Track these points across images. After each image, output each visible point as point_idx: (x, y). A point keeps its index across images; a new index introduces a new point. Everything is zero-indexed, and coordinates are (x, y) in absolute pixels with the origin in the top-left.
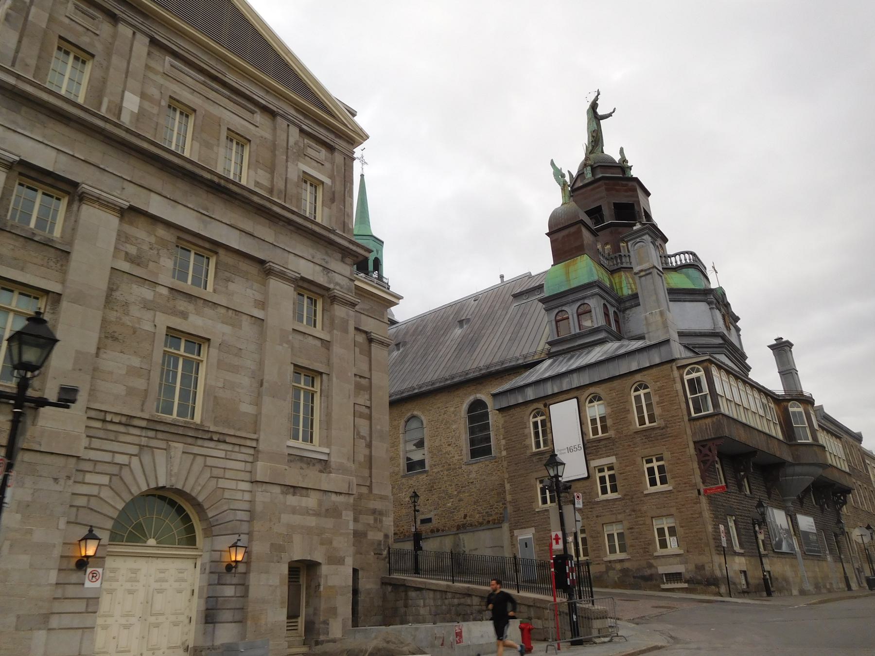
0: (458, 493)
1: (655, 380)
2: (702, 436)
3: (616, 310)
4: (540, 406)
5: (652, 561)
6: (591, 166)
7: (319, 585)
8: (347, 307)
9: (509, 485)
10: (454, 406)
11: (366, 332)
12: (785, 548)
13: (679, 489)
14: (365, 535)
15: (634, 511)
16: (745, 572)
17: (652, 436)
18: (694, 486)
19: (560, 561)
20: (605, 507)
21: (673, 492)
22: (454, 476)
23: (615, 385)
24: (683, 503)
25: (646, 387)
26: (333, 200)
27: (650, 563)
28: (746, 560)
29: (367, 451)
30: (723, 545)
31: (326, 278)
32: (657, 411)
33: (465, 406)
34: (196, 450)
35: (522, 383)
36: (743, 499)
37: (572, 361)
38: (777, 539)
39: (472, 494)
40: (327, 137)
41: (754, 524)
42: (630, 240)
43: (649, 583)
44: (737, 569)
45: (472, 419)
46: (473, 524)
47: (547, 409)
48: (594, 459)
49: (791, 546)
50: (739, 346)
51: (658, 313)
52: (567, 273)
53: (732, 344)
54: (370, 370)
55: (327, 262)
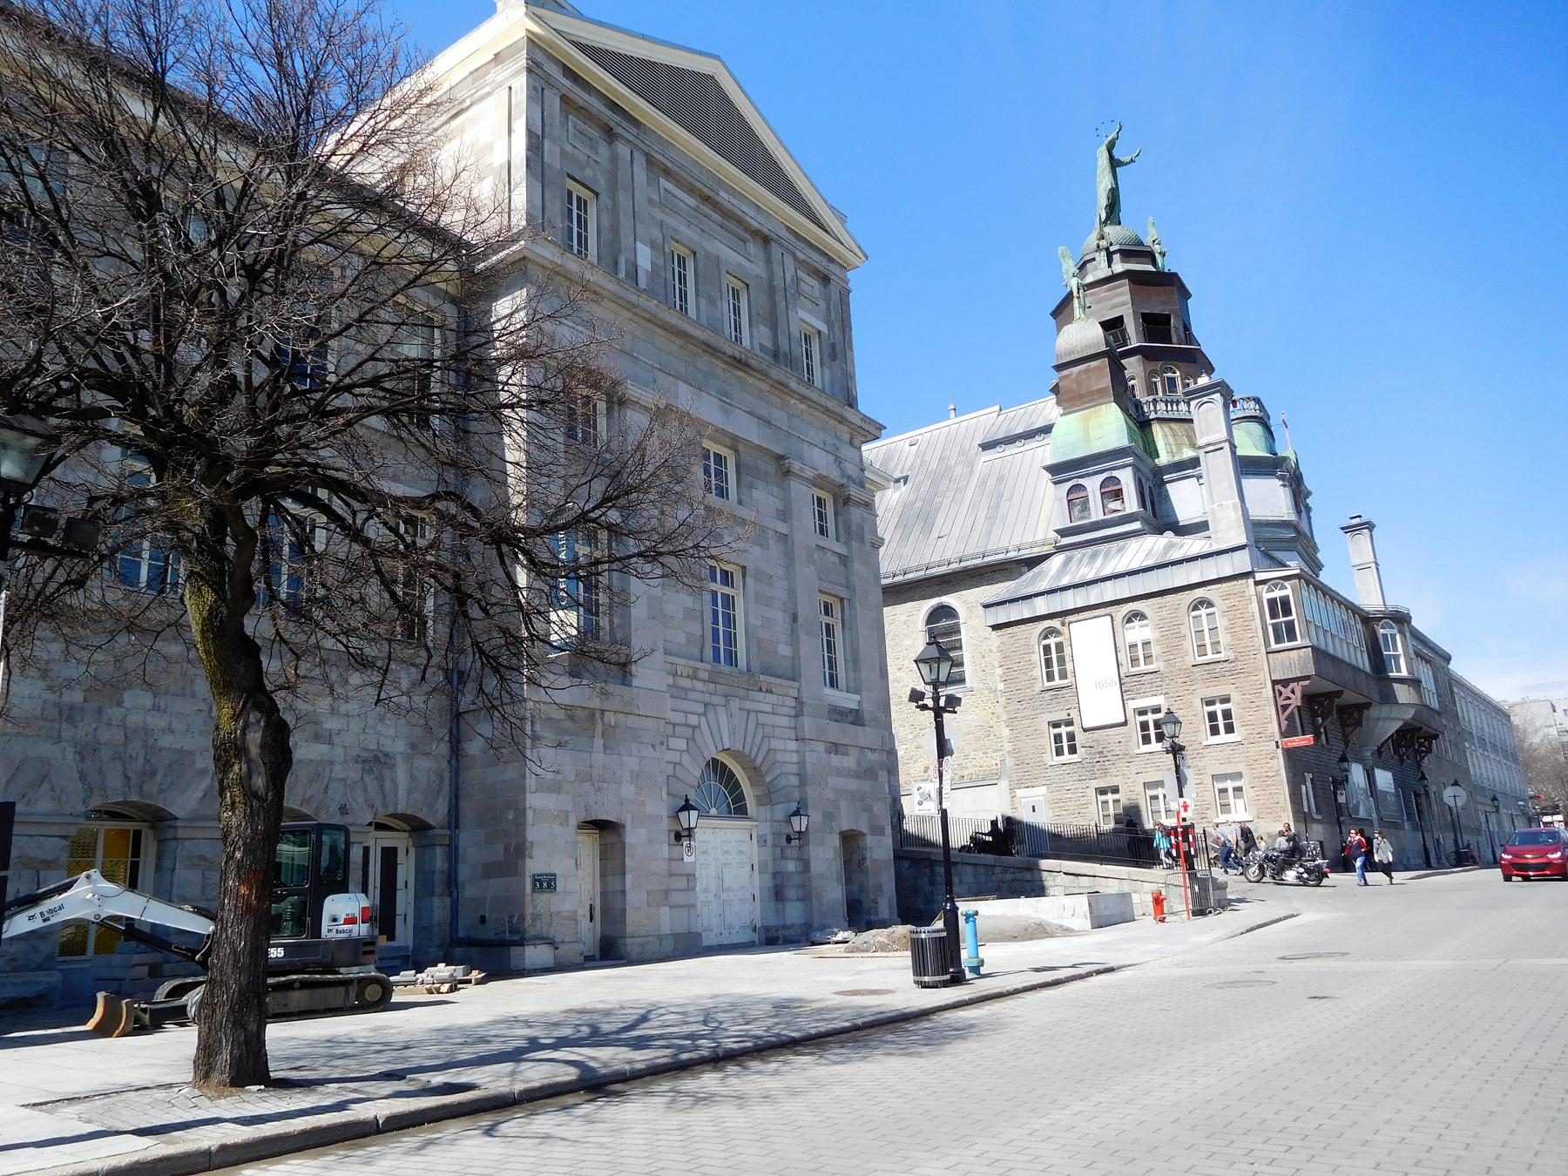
4: (1056, 623)
6: (1107, 249)
7: (864, 859)
9: (1008, 729)
10: (907, 614)
25: (1210, 604)
32: (1224, 638)
34: (749, 705)
37: (1099, 561)
50: (1308, 532)
52: (1087, 429)
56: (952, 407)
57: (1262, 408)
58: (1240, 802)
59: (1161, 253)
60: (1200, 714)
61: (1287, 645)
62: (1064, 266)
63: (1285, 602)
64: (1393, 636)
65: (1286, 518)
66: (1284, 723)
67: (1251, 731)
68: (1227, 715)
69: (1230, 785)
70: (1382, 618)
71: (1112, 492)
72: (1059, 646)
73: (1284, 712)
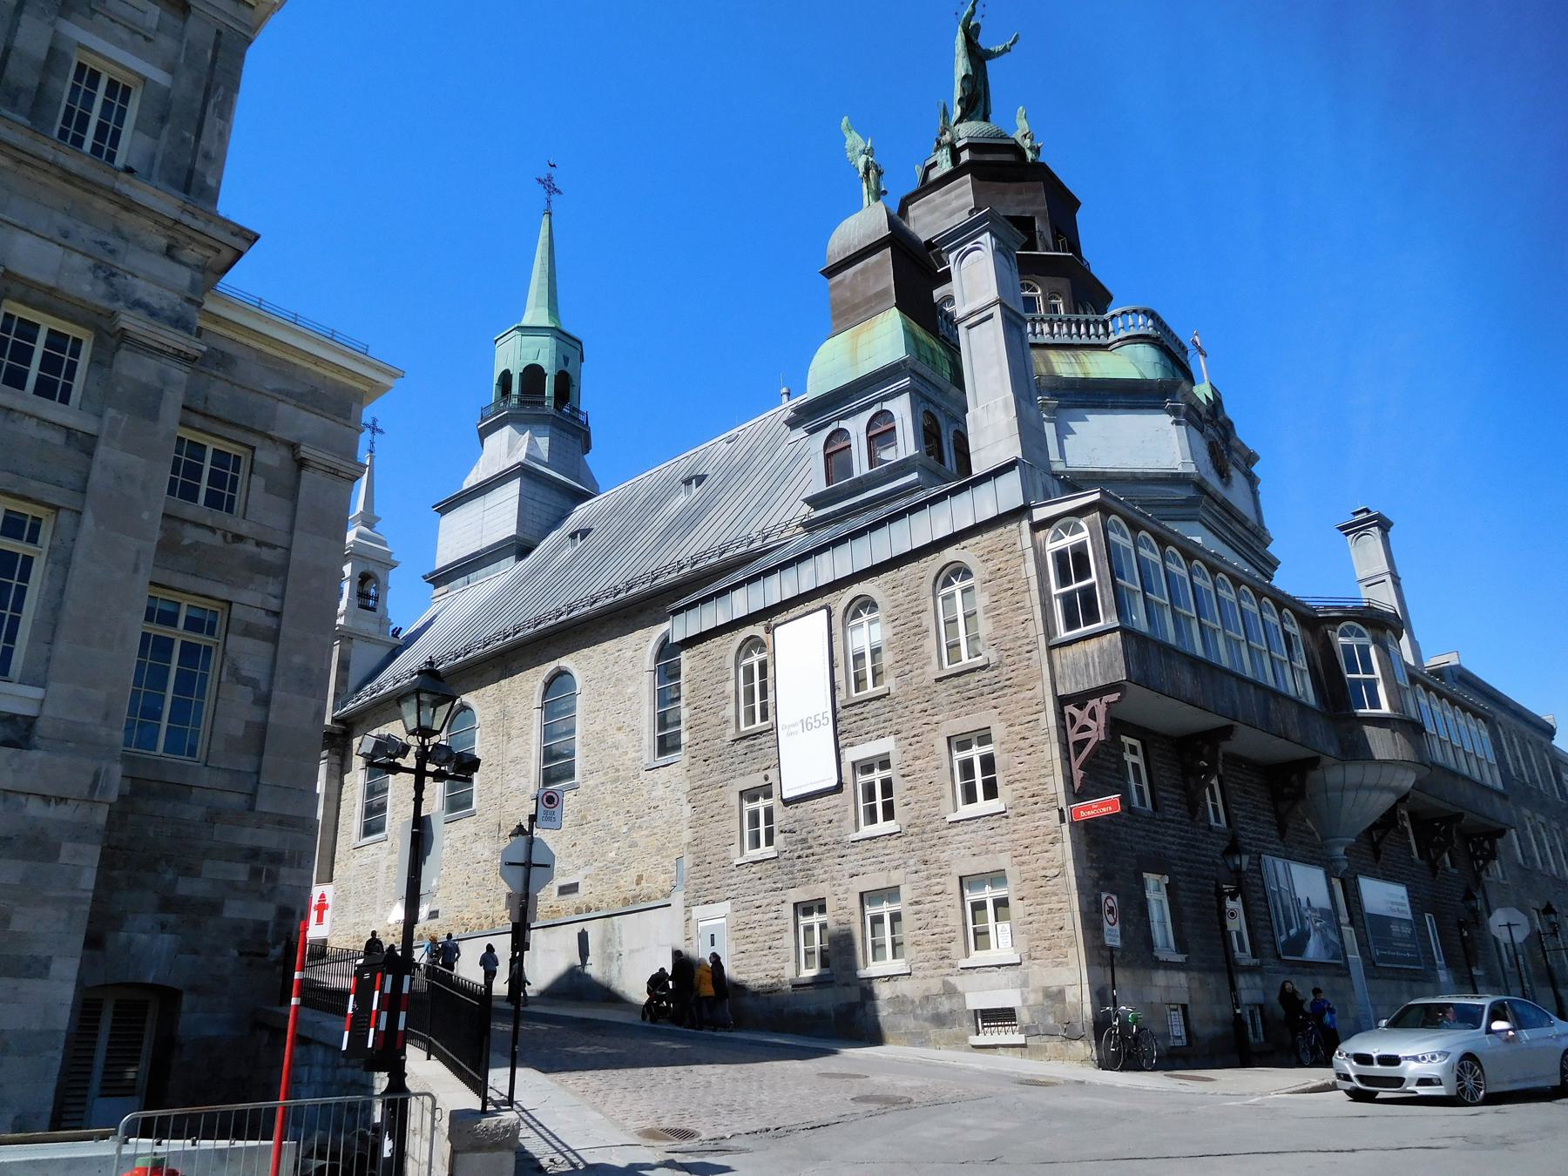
1: (985, 558)
2: (1077, 683)
4: (758, 630)
5: (951, 979)
6: (952, 145)
8: (164, 360)
9: (690, 806)
10: (634, 647)
11: (293, 447)
12: (1313, 951)
13: (1022, 810)
14: (215, 908)
15: (925, 862)
16: (1184, 1007)
17: (971, 687)
18: (1052, 800)
20: (868, 854)
21: (1007, 817)
22: (625, 794)
24: (1027, 842)
25: (967, 573)
26: (163, 119)
28: (1190, 980)
29: (256, 714)
30: (1108, 942)
31: (102, 288)
32: (985, 627)
33: (651, 647)
36: (1201, 837)
38: (1293, 932)
39: (655, 831)
41: (1220, 896)
42: (950, 250)
43: (947, 1031)
44: (1157, 1000)
46: (653, 896)
47: (770, 636)
48: (852, 745)
49: (1341, 951)
50: (1252, 517)
51: (1000, 404)
52: (854, 349)
53: (1227, 507)
54: (291, 532)
55: (112, 252)
56: (784, 390)
57: (1159, 322)
58: (1004, 926)
59: (1031, 148)
60: (946, 765)
61: (1083, 630)
62: (849, 143)
63: (1080, 554)
65: (1180, 470)
66: (1078, 775)
67: (1019, 793)
68: (988, 763)
69: (988, 894)
70: (1339, 620)
71: (881, 435)
72: (763, 666)
73: (1078, 754)
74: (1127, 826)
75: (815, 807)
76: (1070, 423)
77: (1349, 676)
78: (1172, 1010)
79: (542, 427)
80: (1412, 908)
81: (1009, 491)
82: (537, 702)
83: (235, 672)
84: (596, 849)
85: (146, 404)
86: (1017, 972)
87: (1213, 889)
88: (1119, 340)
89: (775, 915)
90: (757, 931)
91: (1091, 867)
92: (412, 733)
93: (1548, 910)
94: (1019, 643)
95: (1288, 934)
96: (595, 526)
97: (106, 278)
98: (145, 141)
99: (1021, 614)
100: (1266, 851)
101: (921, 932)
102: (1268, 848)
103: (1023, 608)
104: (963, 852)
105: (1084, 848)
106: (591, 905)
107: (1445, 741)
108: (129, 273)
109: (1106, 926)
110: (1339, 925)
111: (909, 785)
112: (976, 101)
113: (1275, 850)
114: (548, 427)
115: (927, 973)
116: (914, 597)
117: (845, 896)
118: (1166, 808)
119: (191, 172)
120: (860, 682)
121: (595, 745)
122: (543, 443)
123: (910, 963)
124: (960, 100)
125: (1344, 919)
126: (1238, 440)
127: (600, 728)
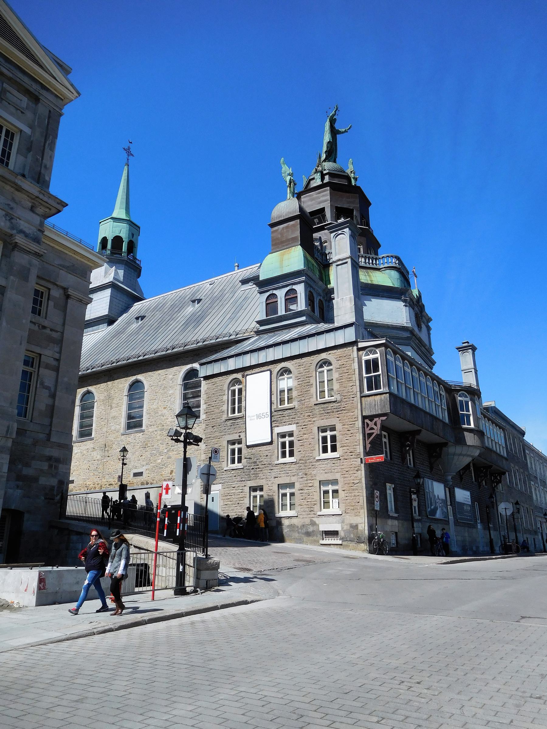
0: (168, 451)
1: (338, 359)
2: (371, 411)
3: (322, 299)
4: (239, 376)
5: (314, 519)
6: (322, 172)
8: (30, 256)
9: (205, 445)
11: (65, 289)
13: (346, 457)
14: (36, 480)
15: (306, 474)
16: (396, 533)
17: (329, 408)
18: (358, 455)
19: (173, 512)
20: (282, 470)
21: (340, 460)
23: (304, 360)
24: (347, 470)
25: (330, 364)
26: (29, 149)
27: (313, 520)
29: (50, 401)
30: (376, 508)
31: (8, 223)
32: (336, 386)
35: (226, 355)
38: (432, 507)
39: (180, 452)
40: (34, 87)
41: (411, 492)
43: (311, 538)
45: (186, 387)
48: (278, 426)
49: (446, 515)
50: (427, 343)
52: (281, 261)
53: (420, 340)
54: (64, 324)
55: (12, 208)
56: (237, 264)
57: (401, 262)
58: (336, 500)
59: (354, 178)
60: (317, 437)
61: (374, 391)
62: (283, 169)
63: (375, 361)
64: (467, 403)
65: (405, 325)
66: (368, 446)
67: (346, 451)
68: (334, 438)
69: (330, 488)
70: (459, 391)
71: (291, 298)
72: (240, 391)
73: (369, 438)
74: (382, 466)
75: (260, 449)
76: (365, 302)
77: (461, 412)
78: (392, 534)
79: (121, 265)
80: (471, 500)
81: (350, 335)
82: (126, 393)
83: (42, 384)
84: (152, 458)
85: (24, 275)
86: (340, 518)
87: (408, 490)
88: (385, 268)
89: (241, 491)
90: (233, 497)
91: (370, 481)
92: (182, 428)
93: (517, 503)
94: (349, 394)
95: (431, 508)
96: (147, 315)
97: (9, 220)
98: (21, 158)
99: (351, 383)
100: (426, 477)
101: (303, 501)
102: (426, 476)
103: (352, 380)
104: (321, 471)
105: (368, 473)
106: (149, 482)
107: (493, 440)
108: (18, 218)
109: (375, 502)
110: (447, 505)
111: (301, 444)
112: (331, 154)
113: (429, 476)
114: (123, 266)
115: (304, 516)
116: (307, 370)
117: (272, 485)
118: (395, 459)
119: (40, 173)
120: (282, 402)
121: (153, 414)
122: (121, 273)
123: (298, 512)
124: (326, 151)
125: (449, 503)
126: (426, 312)
127: (156, 407)
